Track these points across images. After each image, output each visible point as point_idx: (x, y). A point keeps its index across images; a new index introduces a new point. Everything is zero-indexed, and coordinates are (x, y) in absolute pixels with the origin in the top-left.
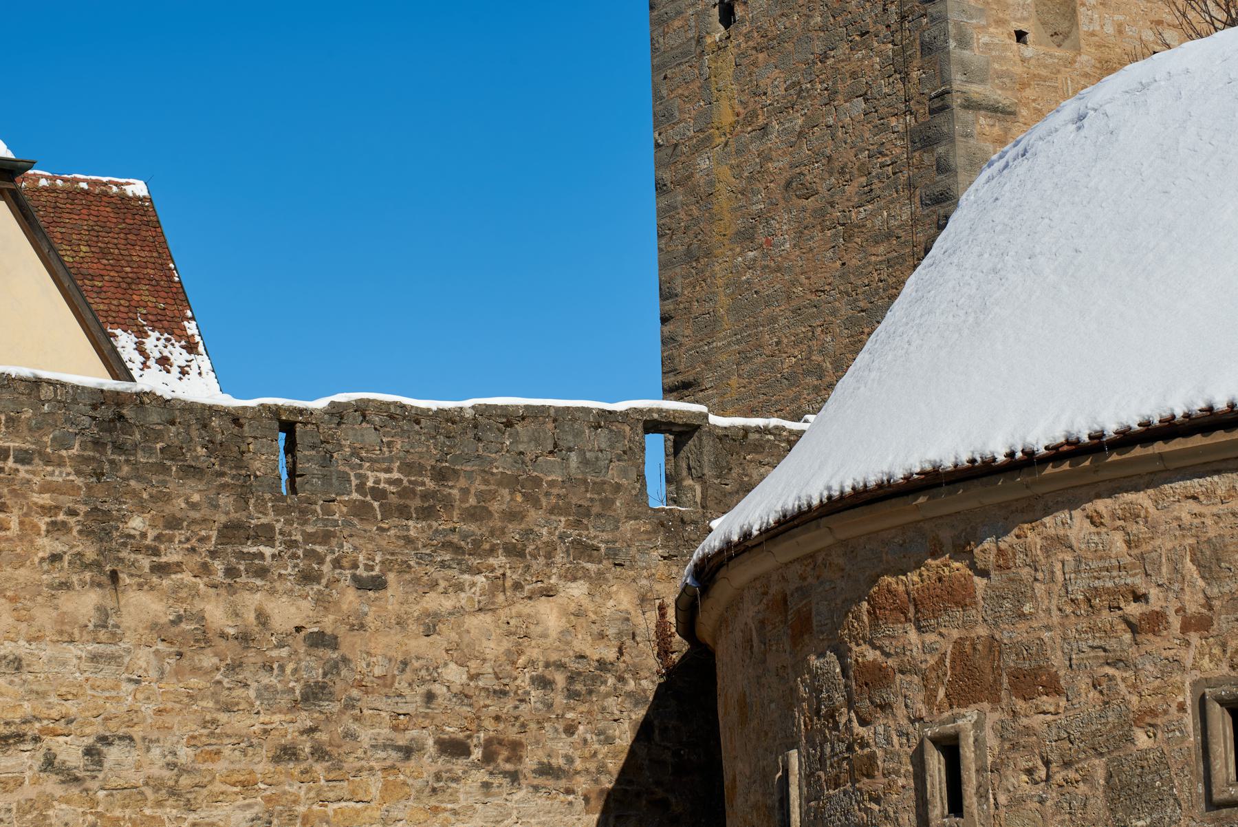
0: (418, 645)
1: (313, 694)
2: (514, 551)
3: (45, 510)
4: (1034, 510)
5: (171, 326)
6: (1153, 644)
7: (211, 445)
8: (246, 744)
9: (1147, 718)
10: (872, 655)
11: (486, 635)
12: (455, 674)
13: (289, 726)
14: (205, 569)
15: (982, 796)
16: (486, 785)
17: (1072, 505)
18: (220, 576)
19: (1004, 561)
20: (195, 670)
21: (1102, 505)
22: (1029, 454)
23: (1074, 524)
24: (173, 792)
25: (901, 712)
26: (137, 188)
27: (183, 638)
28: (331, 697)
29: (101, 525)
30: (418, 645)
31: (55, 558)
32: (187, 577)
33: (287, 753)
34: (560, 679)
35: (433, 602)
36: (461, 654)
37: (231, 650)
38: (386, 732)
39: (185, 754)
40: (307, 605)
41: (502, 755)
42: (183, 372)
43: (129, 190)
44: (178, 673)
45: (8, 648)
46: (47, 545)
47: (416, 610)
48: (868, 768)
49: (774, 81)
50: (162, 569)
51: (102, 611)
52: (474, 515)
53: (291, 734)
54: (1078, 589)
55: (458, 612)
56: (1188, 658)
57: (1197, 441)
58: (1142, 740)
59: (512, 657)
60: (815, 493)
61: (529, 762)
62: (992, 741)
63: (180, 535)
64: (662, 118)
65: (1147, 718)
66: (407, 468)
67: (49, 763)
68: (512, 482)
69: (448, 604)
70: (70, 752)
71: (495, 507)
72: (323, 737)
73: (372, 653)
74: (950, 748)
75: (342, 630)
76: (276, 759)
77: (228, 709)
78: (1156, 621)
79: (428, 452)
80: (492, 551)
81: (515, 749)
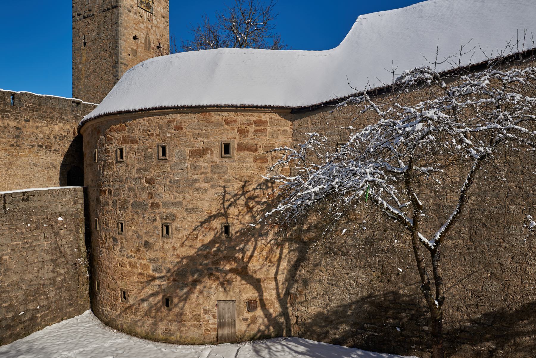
0: (35, 130)
1: (17, 137)
2: (50, 118)
4: (135, 118)
6: (151, 137)
8: (5, 143)
9: (150, 147)
10: (110, 136)
12: (41, 135)
13: (13, 141)
15: (126, 156)
16: (46, 152)
17: (141, 118)
19: (131, 125)
21: (145, 118)
22: (135, 110)
23: (141, 121)
25: (114, 144)
28: (20, 137)
30: (35, 130)
33: (12, 145)
34: (58, 137)
35: (37, 124)
36: (42, 132)
40: (16, 123)
41: (48, 148)
47: (35, 125)
48: (109, 152)
52: (44, 112)
53: (13, 142)
54: (141, 129)
55: (42, 126)
57: (160, 111)
58: (149, 150)
59: (50, 133)
60: (102, 113)
61: (53, 149)
62: (127, 149)
65: (150, 147)
66: (33, 104)
68: (51, 108)
69: (40, 125)
72: (18, 143)
73: (27, 131)
74: (121, 150)
75: (22, 127)
76: (10, 146)
78: (152, 135)
79: (38, 102)
81: (50, 147)
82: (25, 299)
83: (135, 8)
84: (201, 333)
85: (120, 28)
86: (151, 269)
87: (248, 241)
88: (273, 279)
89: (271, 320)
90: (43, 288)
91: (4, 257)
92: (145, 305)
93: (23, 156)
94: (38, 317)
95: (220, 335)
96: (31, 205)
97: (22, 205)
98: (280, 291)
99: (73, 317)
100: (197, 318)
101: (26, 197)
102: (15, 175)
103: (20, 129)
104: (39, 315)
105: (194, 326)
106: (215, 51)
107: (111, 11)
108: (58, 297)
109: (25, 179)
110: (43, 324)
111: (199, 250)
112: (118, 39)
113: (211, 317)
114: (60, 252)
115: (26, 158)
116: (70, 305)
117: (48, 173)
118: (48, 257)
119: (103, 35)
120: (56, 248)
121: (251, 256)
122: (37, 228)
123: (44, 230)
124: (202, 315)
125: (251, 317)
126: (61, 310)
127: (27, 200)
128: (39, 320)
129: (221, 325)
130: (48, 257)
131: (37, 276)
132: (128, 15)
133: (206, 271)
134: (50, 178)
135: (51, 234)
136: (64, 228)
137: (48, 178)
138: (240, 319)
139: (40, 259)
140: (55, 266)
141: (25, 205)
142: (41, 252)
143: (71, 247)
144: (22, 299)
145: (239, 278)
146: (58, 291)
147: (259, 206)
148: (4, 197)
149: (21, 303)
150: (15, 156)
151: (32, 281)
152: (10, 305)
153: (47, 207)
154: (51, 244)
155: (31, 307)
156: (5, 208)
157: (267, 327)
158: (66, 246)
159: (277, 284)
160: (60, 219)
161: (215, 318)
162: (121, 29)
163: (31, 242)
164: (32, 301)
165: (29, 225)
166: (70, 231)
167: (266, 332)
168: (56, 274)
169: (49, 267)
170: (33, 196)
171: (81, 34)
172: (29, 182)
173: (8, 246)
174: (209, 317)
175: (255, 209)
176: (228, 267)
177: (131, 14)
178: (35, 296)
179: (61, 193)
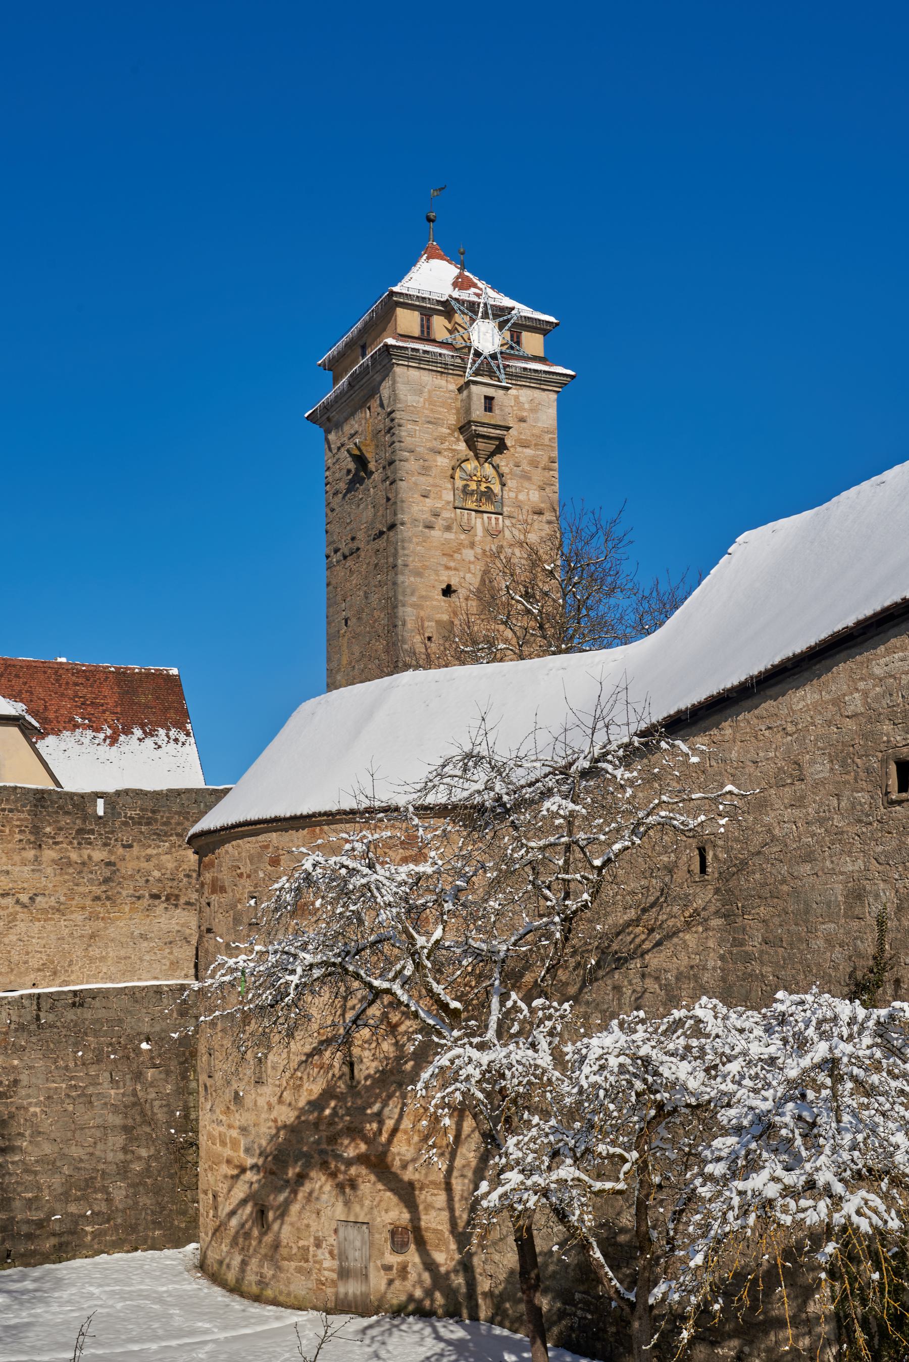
0: (144, 865)
1: (106, 881)
2: (178, 835)
3: (18, 826)
4: (223, 842)
5: (180, 726)
7: (74, 805)
8: (83, 895)
9: (239, 901)
11: (169, 863)
12: (156, 874)
13: (97, 890)
14: (71, 843)
18: (76, 845)
20: (67, 874)
23: (228, 847)
24: (58, 910)
26: (174, 671)
27: (63, 864)
28: (113, 881)
29: (36, 830)
30: (144, 865)
31: (21, 841)
32: (65, 845)
33: (97, 898)
35: (150, 851)
37: (79, 868)
38: (131, 892)
39: (63, 899)
40: (105, 853)
41: (172, 899)
42: (183, 744)
43: (171, 672)
44: (61, 874)
45: (5, 868)
46: (18, 837)
47: (143, 854)
49: (357, 649)
50: (56, 843)
51: (36, 857)
52: (164, 824)
53: (99, 892)
55: (158, 854)
56: (247, 884)
58: (239, 906)
61: (182, 901)
63: (62, 833)
64: (329, 660)
66: (142, 810)
67: (18, 902)
68: (179, 813)
69: (155, 852)
70: (24, 898)
71: (173, 821)
73: (128, 868)
77: (77, 885)
78: (242, 874)
79: (150, 804)
80: (171, 835)
81: (177, 897)
82: (66, 1194)
83: (447, 514)
84: (310, 1286)
85: (400, 578)
86: (242, 1149)
87: (390, 1097)
88: (443, 1186)
89: (439, 1280)
90: (103, 1178)
91: (32, 1109)
92: (234, 1222)
93: (118, 919)
94: (87, 1233)
95: (341, 1296)
96: (88, 1014)
97: (70, 1015)
98: (457, 1213)
99: (161, 1250)
101: (79, 1000)
102: (103, 959)
103: (114, 864)
104: (89, 1229)
105: (299, 1270)
106: (387, 679)
107: (385, 536)
108: (130, 1202)
109: (122, 966)
110: (96, 1246)
111: (302, 1111)
112: (395, 607)
113: (327, 1255)
114: (143, 1113)
115: (126, 922)
116: (157, 1224)
117: (171, 953)
118: (116, 1120)
119: (374, 598)
120: (134, 1104)
121: (395, 1131)
122: (99, 1061)
123: (110, 1067)
124: (311, 1249)
125: (398, 1263)
126: (134, 1228)
127: (81, 1005)
128: (89, 1238)
129: (344, 1273)
130: (118, 1120)
131: (92, 1154)
132: (426, 539)
133: (316, 1156)
134: (175, 965)
135: (124, 1076)
136: (155, 1066)
137: (172, 963)
138: (377, 1266)
139: (99, 1121)
140: (131, 1139)
141: (76, 1014)
142: (102, 1109)
143: (168, 1105)
144: (60, 1191)
145: (373, 1178)
146: (131, 1190)
147: (408, 1023)
148: (38, 998)
149: (57, 1198)
150: (103, 919)
151: (81, 1160)
152: (36, 1198)
153: (120, 1021)
154: (124, 1095)
155: (73, 1208)
156: (38, 1018)
157: (429, 1293)
158: (157, 1103)
159: (450, 1199)
160: (144, 1046)
161: (333, 1258)
162: (406, 580)
163: (85, 1088)
164: (78, 1199)
165: (80, 1054)
166: (168, 1073)
167: (427, 1303)
168: (129, 1157)
169: (119, 1140)
170: (94, 998)
171: (339, 598)
172: (132, 972)
173: (39, 1089)
174: (323, 1254)
175: (402, 1028)
176: (351, 1153)
177: (436, 533)
178: (85, 1190)
179: (151, 994)
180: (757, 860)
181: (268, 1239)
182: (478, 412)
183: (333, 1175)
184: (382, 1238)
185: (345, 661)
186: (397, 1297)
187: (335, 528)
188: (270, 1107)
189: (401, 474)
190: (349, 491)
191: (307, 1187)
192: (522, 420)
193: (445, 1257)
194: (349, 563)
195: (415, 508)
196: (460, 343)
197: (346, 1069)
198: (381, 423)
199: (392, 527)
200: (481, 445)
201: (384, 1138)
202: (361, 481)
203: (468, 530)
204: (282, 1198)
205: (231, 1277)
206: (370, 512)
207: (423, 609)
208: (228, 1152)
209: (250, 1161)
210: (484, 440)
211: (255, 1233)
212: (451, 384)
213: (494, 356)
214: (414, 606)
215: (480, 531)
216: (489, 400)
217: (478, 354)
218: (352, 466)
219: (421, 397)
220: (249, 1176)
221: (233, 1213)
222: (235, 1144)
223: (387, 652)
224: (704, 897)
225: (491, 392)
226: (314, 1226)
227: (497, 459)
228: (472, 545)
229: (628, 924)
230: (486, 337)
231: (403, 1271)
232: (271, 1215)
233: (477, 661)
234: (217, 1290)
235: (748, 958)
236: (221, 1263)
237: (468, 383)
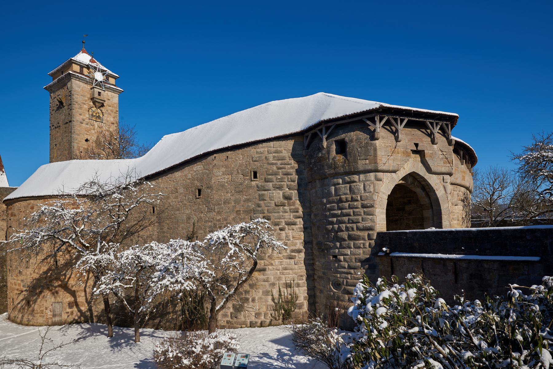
49: (59, 153)
83: (87, 120)
85: (73, 135)
87: (68, 269)
92: (19, 306)
100: (42, 312)
105: (40, 316)
111: (41, 275)
119: (65, 140)
121: (70, 278)
129: (54, 316)
132: (80, 126)
157: (79, 318)
162: (74, 136)
175: (72, 252)
176: (56, 284)
177: (83, 125)
180: (167, 210)
181: (31, 309)
182: (96, 95)
183: (51, 291)
184: (66, 305)
185: (55, 155)
186: (70, 319)
187: (53, 120)
188: (31, 274)
189: (73, 108)
190: (57, 110)
191: (43, 294)
192: (109, 100)
193: (84, 308)
194: (57, 129)
195: (77, 118)
196: (91, 77)
197: (55, 263)
198: (67, 93)
199: (70, 121)
200: (97, 104)
201: (66, 280)
202: (61, 108)
203: (93, 125)
204: (35, 298)
205: (19, 320)
206: (64, 117)
207: (79, 144)
208: (17, 287)
209: (24, 289)
210: (98, 103)
211: (26, 308)
212: (89, 87)
213: (101, 82)
214: (77, 143)
215: (96, 126)
216: (99, 93)
217: (96, 80)
218: (58, 103)
219: (79, 89)
220: (24, 293)
221: (19, 303)
222: (19, 285)
223: (68, 154)
224: (154, 218)
225: (100, 91)
226: (45, 304)
227: (101, 108)
228: (94, 129)
229: (135, 225)
230: (99, 77)
231: (72, 313)
232: (31, 303)
233: (95, 159)
234: (14, 324)
235: (164, 232)
236: (15, 317)
237: (94, 87)
